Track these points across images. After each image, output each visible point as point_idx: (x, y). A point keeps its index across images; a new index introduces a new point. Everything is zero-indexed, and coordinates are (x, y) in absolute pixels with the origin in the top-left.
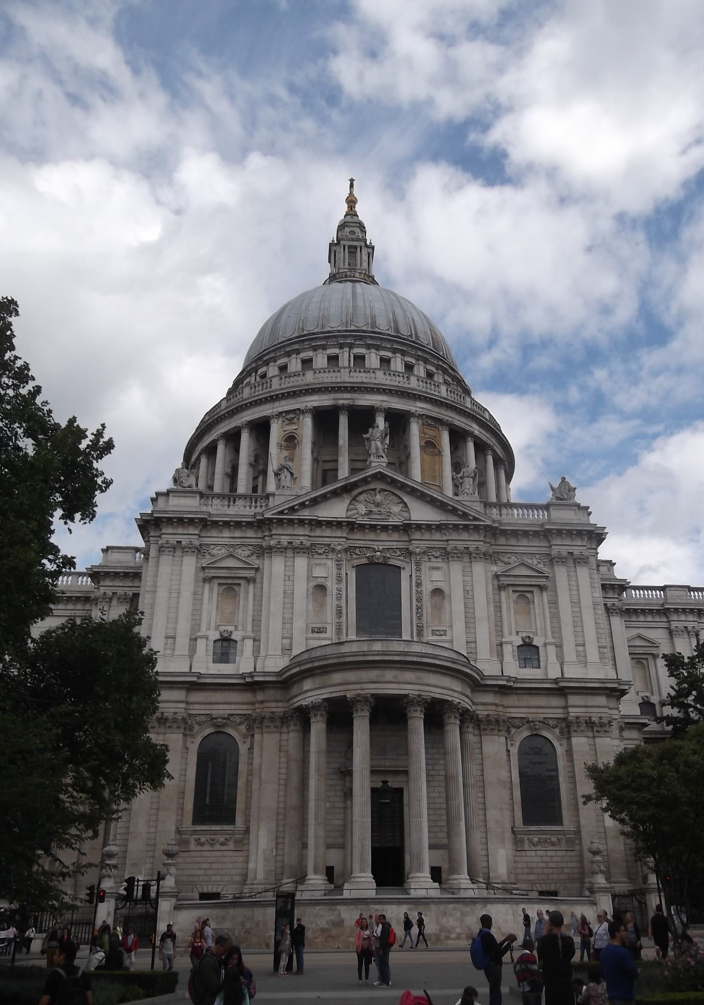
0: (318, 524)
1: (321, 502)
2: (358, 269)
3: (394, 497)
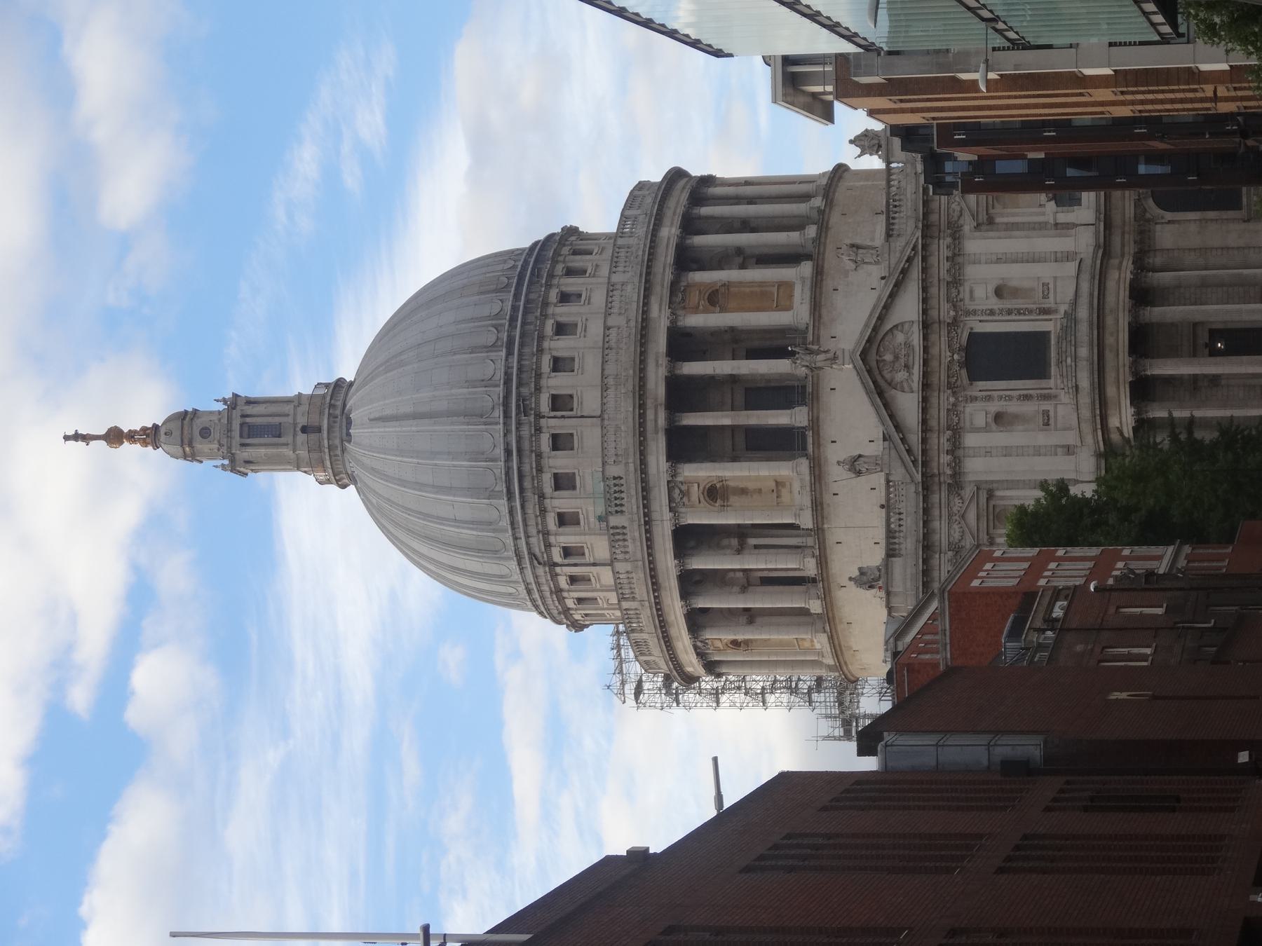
0: (924, 422)
2: (295, 420)
3: (886, 339)
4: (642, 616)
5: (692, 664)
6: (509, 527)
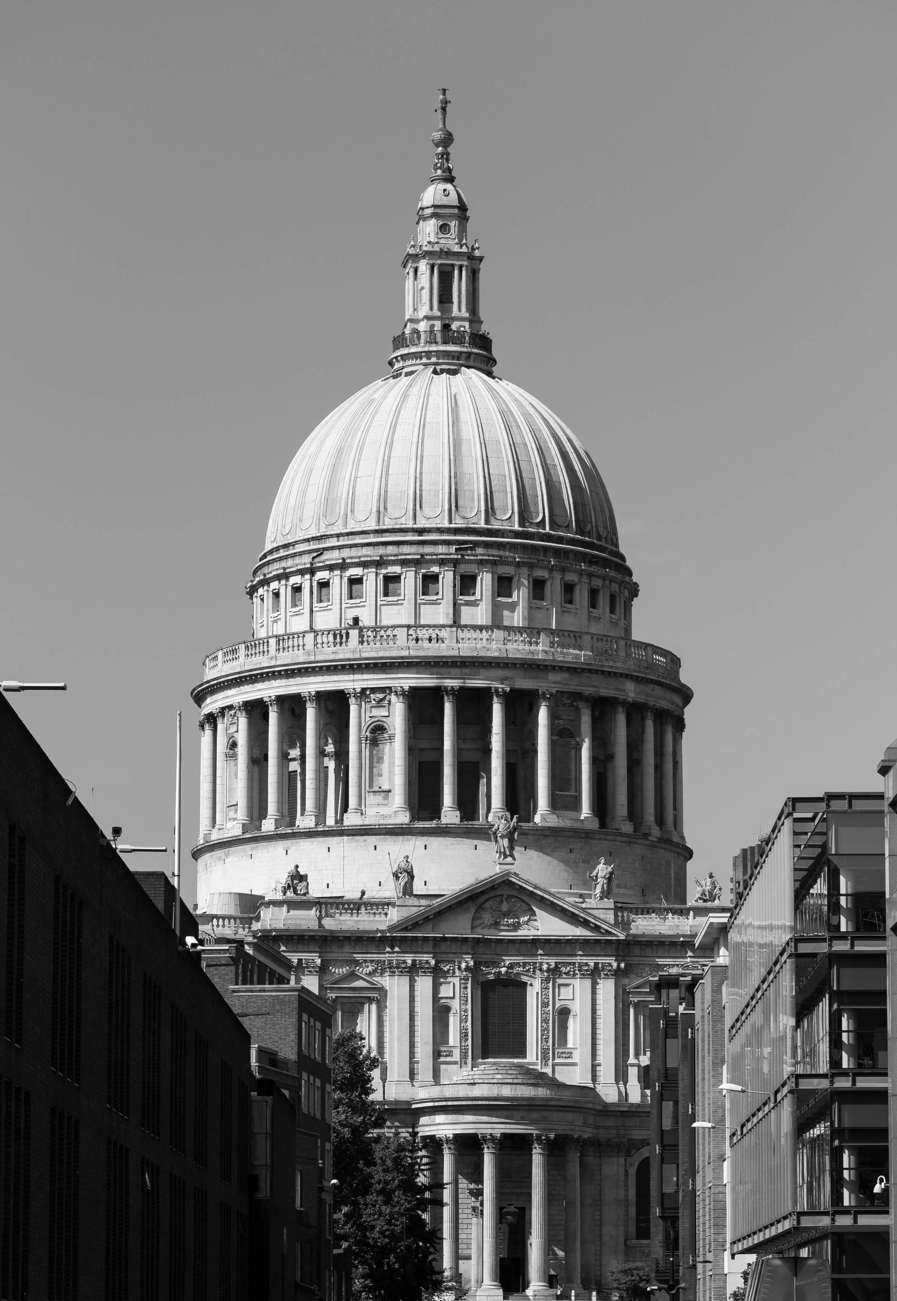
0: (444, 939)
1: (445, 913)
4: (261, 657)
5: (213, 704)
6: (349, 530)
